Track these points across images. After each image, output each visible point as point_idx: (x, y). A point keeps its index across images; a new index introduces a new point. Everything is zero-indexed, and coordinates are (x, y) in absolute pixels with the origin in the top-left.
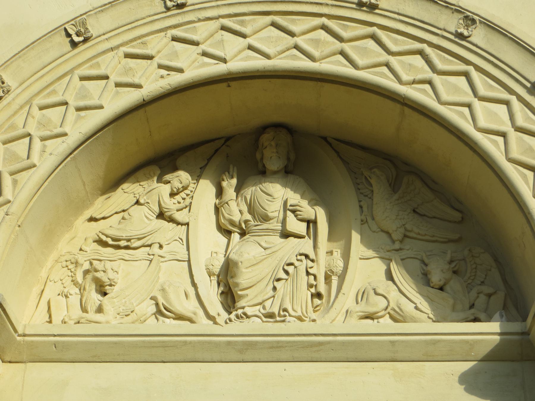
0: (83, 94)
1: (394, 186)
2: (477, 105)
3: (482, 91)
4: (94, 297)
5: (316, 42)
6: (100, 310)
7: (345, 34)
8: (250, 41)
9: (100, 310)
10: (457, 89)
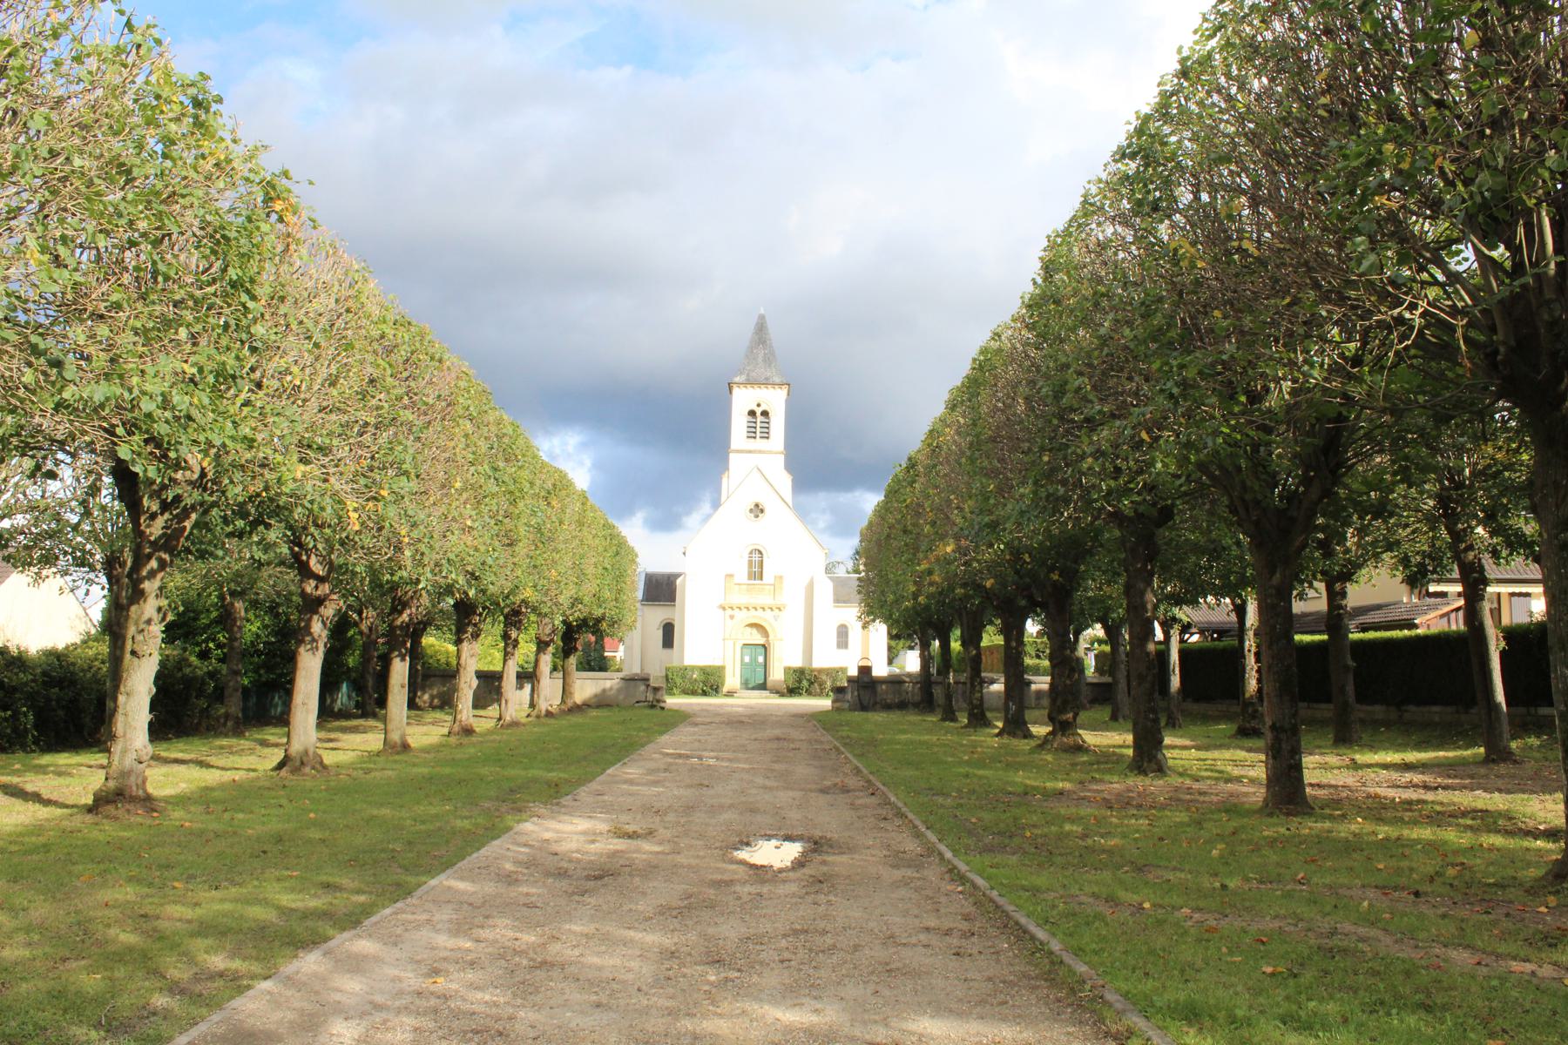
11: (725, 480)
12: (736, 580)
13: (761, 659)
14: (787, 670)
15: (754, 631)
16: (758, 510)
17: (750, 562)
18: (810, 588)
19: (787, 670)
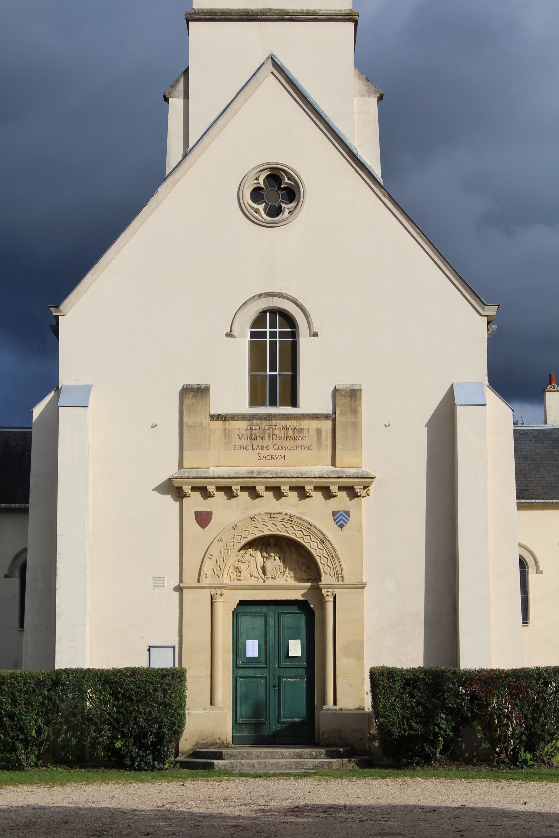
0: (237, 539)
1: (297, 549)
2: (311, 542)
3: (313, 540)
4: (239, 574)
5: (281, 528)
6: (240, 576)
7: (287, 526)
8: (269, 527)
9: (240, 576)
10: (307, 539)
11: (176, 105)
12: (217, 404)
13: (295, 648)
14: (383, 680)
15: (274, 563)
16: (277, 192)
17: (257, 351)
18: (443, 428)
19: (381, 679)
